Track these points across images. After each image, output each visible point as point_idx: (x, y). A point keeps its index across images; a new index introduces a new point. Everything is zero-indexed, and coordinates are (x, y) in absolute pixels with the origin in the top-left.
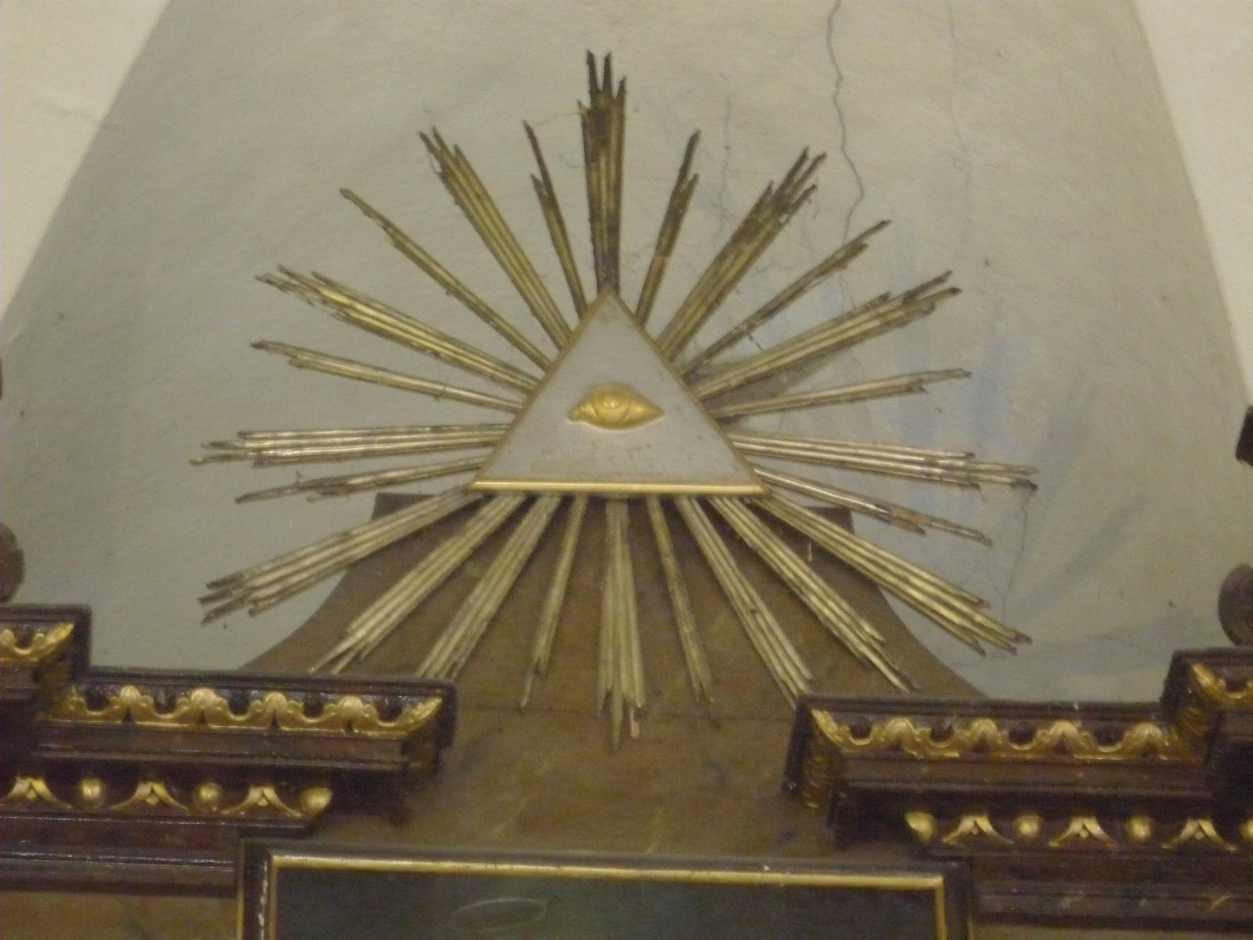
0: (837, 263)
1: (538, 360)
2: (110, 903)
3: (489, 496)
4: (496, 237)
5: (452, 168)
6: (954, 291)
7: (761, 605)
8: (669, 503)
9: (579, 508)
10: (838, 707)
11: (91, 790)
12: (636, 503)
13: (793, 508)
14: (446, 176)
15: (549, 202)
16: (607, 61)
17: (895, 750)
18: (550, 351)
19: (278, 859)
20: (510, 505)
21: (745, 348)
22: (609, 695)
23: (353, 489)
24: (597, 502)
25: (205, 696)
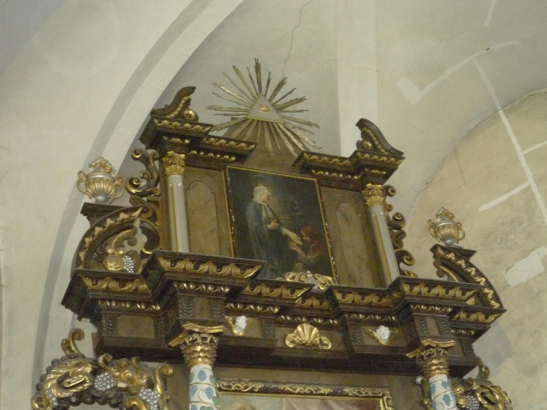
0: (290, 93)
1: (252, 101)
2: (204, 170)
3: (248, 119)
4: (244, 82)
5: (237, 71)
8: (272, 123)
9: (260, 123)
11: (202, 153)
12: (267, 123)
13: (290, 127)
14: (237, 73)
15: (251, 78)
17: (313, 160)
19: (228, 167)
21: (279, 103)
24: (262, 122)
25: (223, 141)
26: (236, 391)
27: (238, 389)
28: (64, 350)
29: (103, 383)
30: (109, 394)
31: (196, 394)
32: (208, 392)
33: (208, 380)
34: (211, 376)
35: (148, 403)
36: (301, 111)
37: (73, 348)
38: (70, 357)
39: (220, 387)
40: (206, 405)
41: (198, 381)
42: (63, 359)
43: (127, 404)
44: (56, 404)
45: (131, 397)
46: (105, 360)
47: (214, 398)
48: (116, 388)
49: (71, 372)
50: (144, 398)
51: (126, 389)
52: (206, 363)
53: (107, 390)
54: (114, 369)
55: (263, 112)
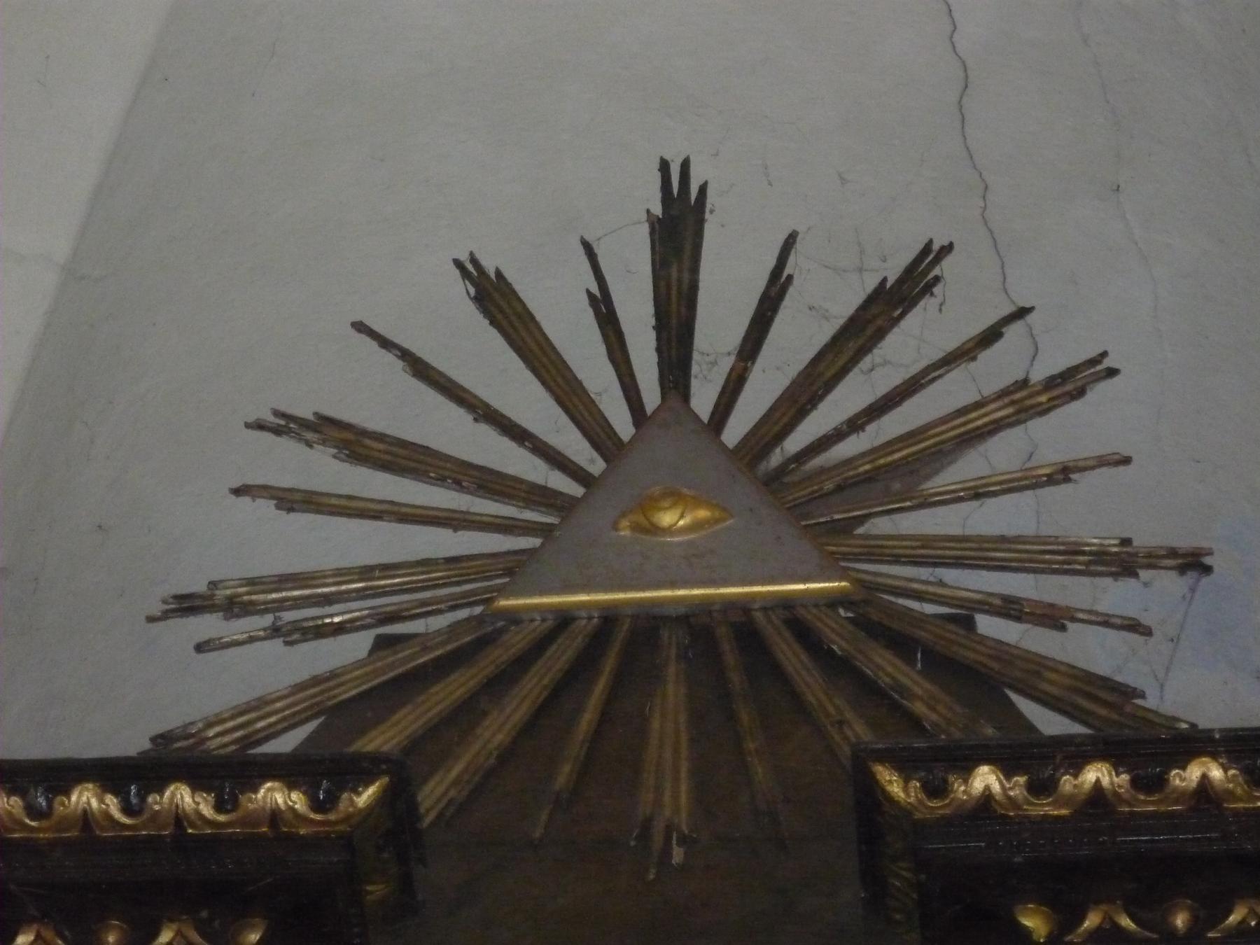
5: (495, 297)
6: (1112, 372)
7: (849, 715)
10: (905, 764)
16: (685, 165)
18: (596, 466)
20: (539, 626)
22: (647, 824)
23: (339, 629)
24: (649, 624)
36: (1064, 474)
55: (692, 554)
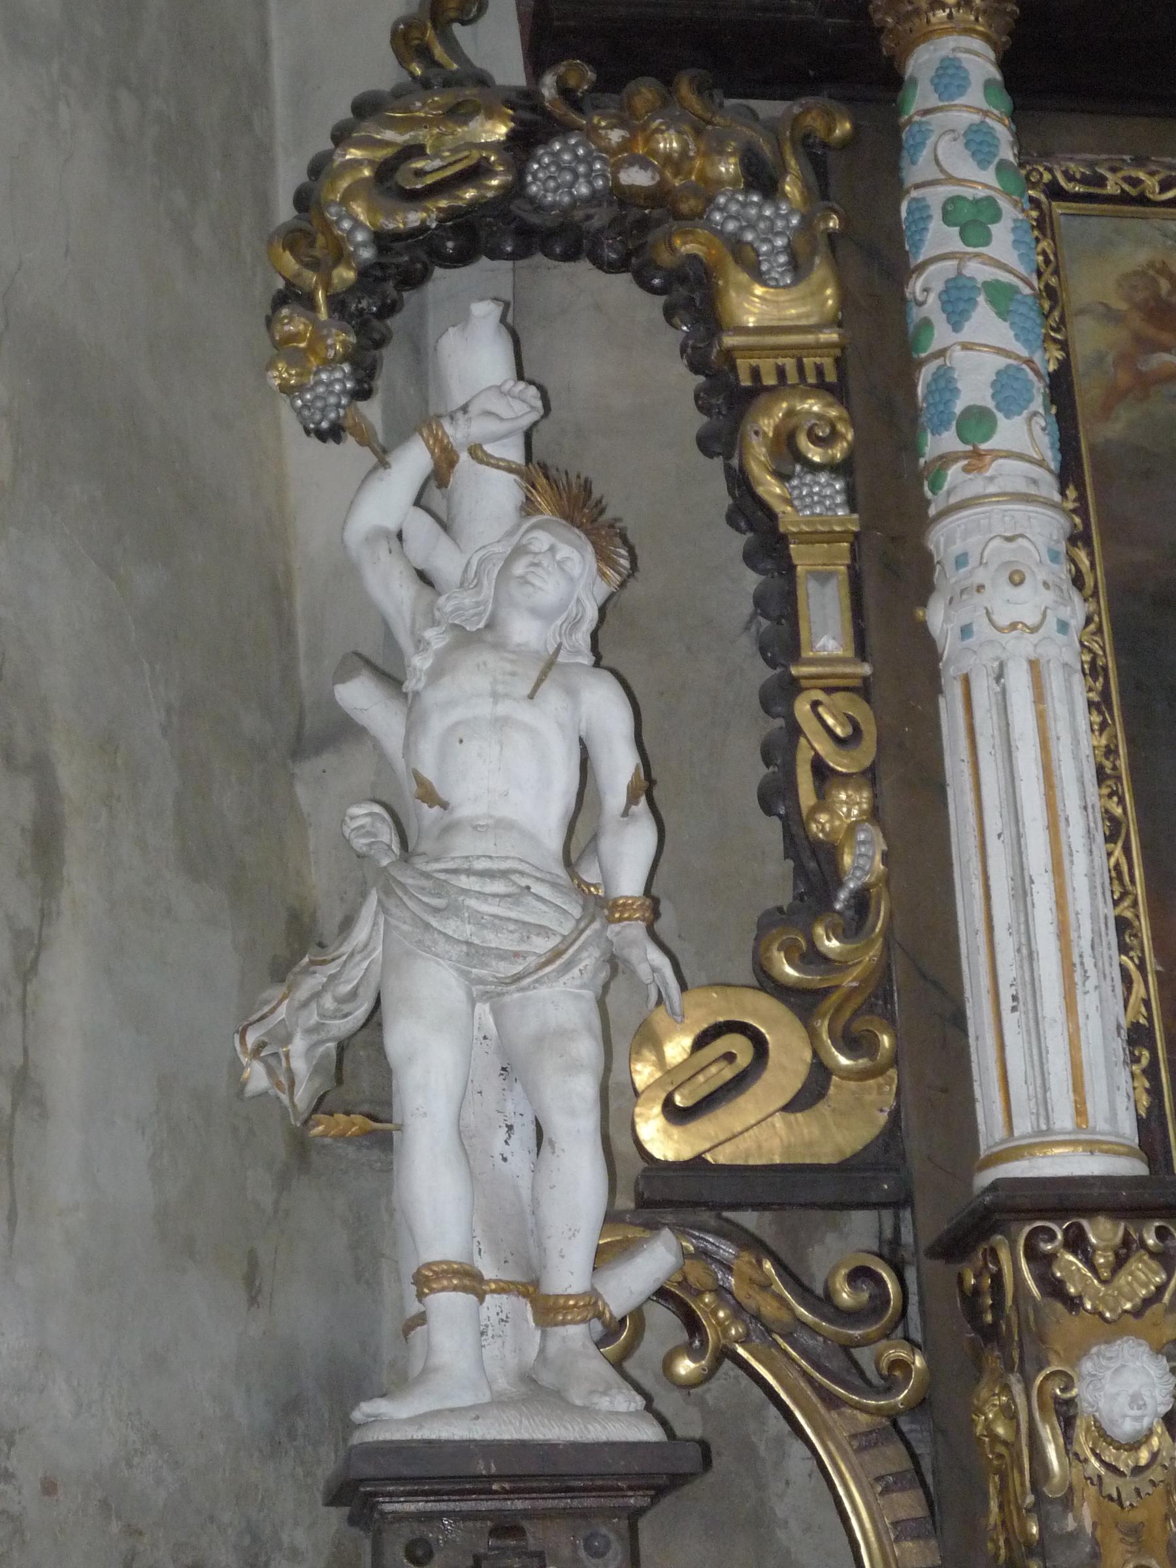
26: (1123, 199)
27: (1133, 192)
28: (403, 62)
29: (562, 177)
30: (589, 217)
31: (925, 154)
32: (977, 143)
33: (975, 96)
34: (988, 84)
35: (750, 244)
37: (439, 52)
38: (425, 84)
39: (1054, 181)
40: (968, 192)
41: (933, 101)
42: (398, 93)
43: (665, 258)
44: (367, 254)
45: (675, 226)
46: (565, 92)
47: (1002, 166)
48: (622, 196)
49: (424, 136)
50: (731, 226)
51: (659, 196)
52: (968, 31)
53: (576, 202)
54: (603, 117)
